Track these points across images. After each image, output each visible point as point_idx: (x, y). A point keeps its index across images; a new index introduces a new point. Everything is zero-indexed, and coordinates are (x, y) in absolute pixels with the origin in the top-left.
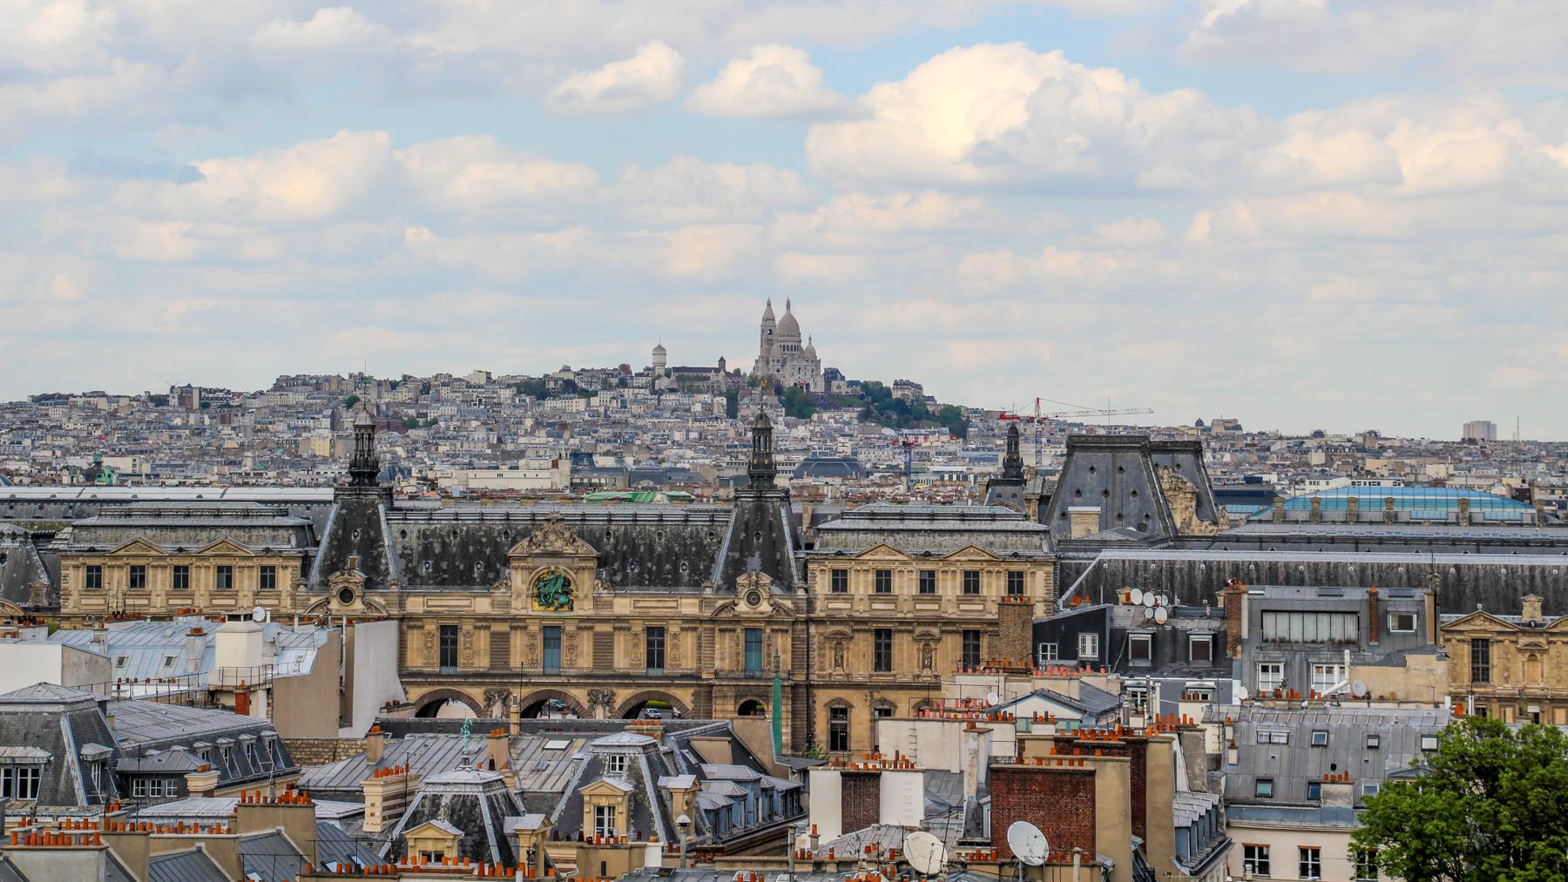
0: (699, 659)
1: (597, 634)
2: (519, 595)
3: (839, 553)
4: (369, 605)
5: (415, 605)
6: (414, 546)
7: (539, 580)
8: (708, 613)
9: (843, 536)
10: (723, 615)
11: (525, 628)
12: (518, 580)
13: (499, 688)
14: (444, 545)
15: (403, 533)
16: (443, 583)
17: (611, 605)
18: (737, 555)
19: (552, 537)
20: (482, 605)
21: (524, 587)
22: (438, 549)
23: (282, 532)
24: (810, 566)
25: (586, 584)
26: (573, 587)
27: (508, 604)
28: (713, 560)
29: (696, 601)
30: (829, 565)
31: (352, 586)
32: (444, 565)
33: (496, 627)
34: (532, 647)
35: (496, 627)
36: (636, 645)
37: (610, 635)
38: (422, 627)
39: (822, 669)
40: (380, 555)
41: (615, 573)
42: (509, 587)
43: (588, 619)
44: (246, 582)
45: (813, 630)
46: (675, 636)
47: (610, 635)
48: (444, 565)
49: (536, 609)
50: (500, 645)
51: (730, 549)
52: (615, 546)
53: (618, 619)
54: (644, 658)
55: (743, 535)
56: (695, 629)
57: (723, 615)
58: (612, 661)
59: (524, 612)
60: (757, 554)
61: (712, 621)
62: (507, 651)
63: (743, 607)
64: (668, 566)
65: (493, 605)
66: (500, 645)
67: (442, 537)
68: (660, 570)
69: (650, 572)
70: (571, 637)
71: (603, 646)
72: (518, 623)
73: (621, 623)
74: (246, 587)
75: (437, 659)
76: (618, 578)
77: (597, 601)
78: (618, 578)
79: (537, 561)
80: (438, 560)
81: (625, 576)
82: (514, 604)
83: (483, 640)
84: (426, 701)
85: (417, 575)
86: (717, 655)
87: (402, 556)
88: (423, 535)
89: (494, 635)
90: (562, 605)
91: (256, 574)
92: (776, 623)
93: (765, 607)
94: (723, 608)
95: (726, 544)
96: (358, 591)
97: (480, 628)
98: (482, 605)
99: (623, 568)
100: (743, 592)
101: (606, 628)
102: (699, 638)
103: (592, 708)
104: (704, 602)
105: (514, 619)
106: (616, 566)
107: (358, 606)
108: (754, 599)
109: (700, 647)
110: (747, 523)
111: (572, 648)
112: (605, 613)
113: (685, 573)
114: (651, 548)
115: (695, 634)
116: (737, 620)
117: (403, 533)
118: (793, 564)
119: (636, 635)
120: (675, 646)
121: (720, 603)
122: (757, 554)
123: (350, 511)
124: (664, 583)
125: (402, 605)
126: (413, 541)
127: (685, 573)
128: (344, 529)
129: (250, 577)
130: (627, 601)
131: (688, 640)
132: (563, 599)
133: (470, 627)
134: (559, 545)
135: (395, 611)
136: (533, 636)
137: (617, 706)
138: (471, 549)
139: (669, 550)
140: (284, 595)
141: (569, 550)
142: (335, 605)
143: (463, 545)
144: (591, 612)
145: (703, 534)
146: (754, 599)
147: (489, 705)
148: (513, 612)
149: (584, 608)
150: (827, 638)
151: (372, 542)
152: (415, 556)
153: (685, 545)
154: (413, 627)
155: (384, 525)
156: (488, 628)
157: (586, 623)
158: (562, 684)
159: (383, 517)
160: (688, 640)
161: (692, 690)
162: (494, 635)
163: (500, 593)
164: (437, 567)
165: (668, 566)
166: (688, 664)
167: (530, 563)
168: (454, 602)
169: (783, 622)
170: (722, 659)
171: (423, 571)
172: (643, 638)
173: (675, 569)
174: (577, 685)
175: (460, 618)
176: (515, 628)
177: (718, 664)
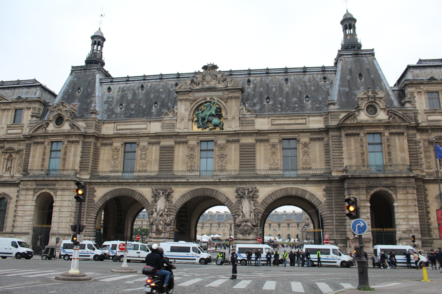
0: (328, 162)
1: (242, 146)
2: (182, 120)
3: (432, 79)
4: (73, 126)
5: (108, 129)
6: (115, 95)
7: (197, 109)
8: (334, 123)
9: (428, 71)
10: (348, 122)
11: (186, 142)
12: (183, 109)
13: (163, 187)
14: (134, 94)
15: (109, 89)
16: (131, 116)
17: (253, 123)
18: (347, 89)
19: (208, 78)
20: (155, 127)
21: (187, 113)
22: (130, 96)
23: (34, 90)
24: (409, 90)
25: (233, 109)
26: (223, 113)
27: (173, 126)
28: (328, 94)
29: (321, 119)
30: (425, 88)
31: (64, 114)
32: (133, 106)
33: (165, 142)
34: (191, 157)
35: (165, 142)
36: (274, 153)
37: (253, 146)
38: (111, 144)
39: (429, 168)
40: (92, 102)
41: (255, 105)
42: (175, 114)
43: (236, 134)
44: (4, 119)
45: (418, 137)
46: (305, 145)
47: (253, 146)
48: (133, 106)
49: (195, 129)
50: (167, 157)
51: (340, 86)
52: (254, 89)
53: (259, 133)
54: (280, 163)
55: (349, 77)
56: (322, 139)
57: (348, 122)
58: (254, 166)
59: (186, 130)
60: (362, 88)
61: (339, 128)
62: (171, 160)
63: (363, 116)
64: (294, 99)
65: (163, 127)
66: (167, 157)
67: (134, 91)
68: (288, 102)
69: (281, 103)
70: (222, 148)
71: (247, 156)
72: (181, 138)
73: (261, 136)
74: (4, 122)
75: (120, 168)
76: (257, 108)
77: (242, 120)
78: (257, 108)
79: (197, 95)
80: (129, 103)
81: (263, 107)
82: (178, 126)
83: (154, 153)
84: (108, 198)
85: (113, 113)
86: (345, 155)
87: (106, 102)
88: (123, 90)
89: (162, 148)
90: (216, 126)
91: (11, 114)
92: (394, 127)
93: (382, 116)
94: (346, 118)
95: (337, 82)
96: (66, 116)
97: (153, 144)
98: (155, 127)
99: (261, 102)
100: (363, 105)
101: (250, 140)
102: (327, 145)
103: (240, 202)
104: (327, 115)
105: (177, 135)
106: (255, 100)
107: (66, 127)
108: (372, 109)
109: (327, 152)
110: (350, 70)
111: (222, 157)
112: (248, 128)
113: (309, 104)
114: (281, 89)
115: (321, 143)
116: (361, 126)
117: (109, 89)
118: (391, 93)
119: (274, 146)
120: (306, 153)
121: (343, 115)
122: (362, 88)
123: (79, 78)
124: (294, 109)
125: (98, 128)
126: (115, 93)
127: (309, 104)
128: (73, 88)
129: (7, 116)
130: (266, 120)
131: (317, 149)
132: (216, 121)
133: (145, 144)
134: (213, 83)
135: (91, 131)
136: (192, 149)
137: (260, 200)
138: (152, 96)
139: (294, 90)
140: (25, 126)
141: (221, 86)
142: (51, 128)
143: (147, 94)
144: (238, 129)
145: (318, 79)
146: (372, 109)
147: (156, 201)
148: (177, 130)
149: (231, 125)
150: (430, 142)
151: (89, 95)
152: (115, 102)
153: (306, 86)
154: (106, 145)
155: (97, 84)
156: (159, 143)
157: (235, 136)
158: (214, 183)
159: (97, 81)
160: (317, 149)
161: (324, 187)
162: (162, 148)
163: (167, 119)
164: (127, 108)
165: (294, 99)
166: (318, 166)
167: (191, 96)
168: (137, 126)
169: (399, 126)
170: (350, 158)
171: (118, 110)
172: (279, 147)
173: (301, 101)
174: (226, 184)
175: (139, 136)
176: (179, 143)
177: (346, 162)
